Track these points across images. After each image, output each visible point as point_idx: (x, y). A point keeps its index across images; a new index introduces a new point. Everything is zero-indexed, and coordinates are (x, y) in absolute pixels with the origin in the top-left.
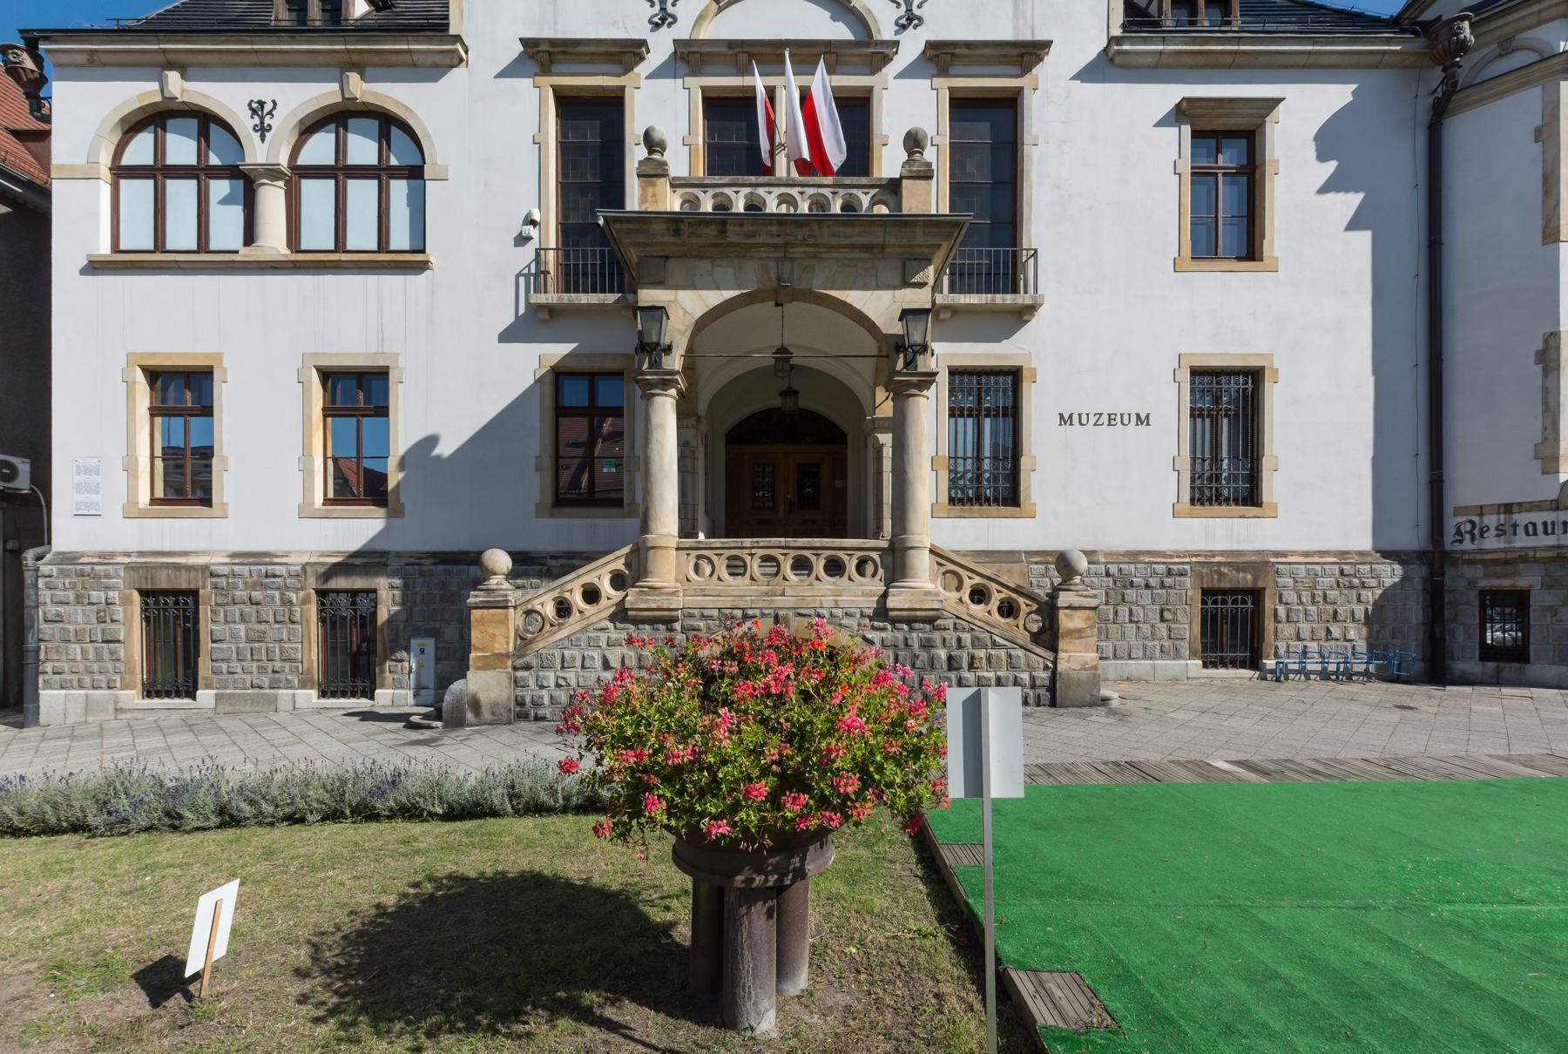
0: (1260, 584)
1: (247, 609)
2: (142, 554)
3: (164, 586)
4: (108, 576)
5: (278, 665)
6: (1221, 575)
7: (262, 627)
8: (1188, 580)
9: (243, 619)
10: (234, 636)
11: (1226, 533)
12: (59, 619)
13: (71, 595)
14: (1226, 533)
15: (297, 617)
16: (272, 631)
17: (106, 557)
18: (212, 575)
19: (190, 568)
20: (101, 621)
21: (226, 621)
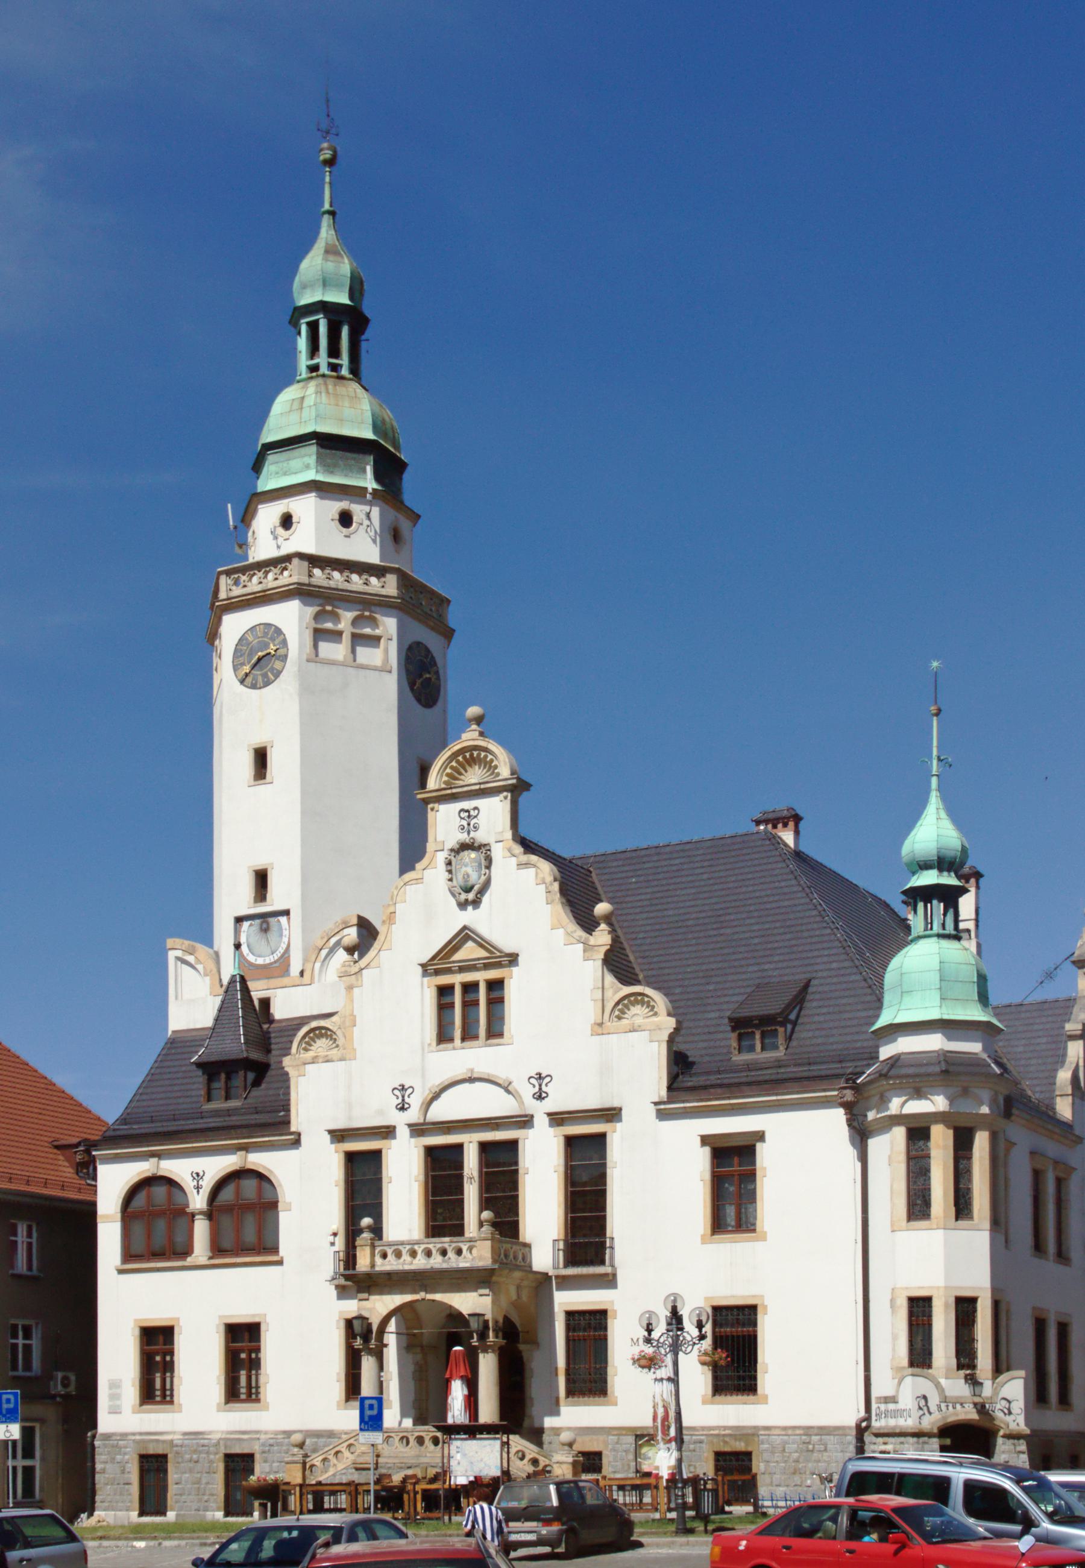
0: (749, 1449)
2: (141, 1434)
3: (151, 1452)
6: (725, 1442)
8: (704, 1445)
11: (734, 1414)
12: (103, 1471)
14: (734, 1414)
17: (124, 1436)
19: (164, 1442)
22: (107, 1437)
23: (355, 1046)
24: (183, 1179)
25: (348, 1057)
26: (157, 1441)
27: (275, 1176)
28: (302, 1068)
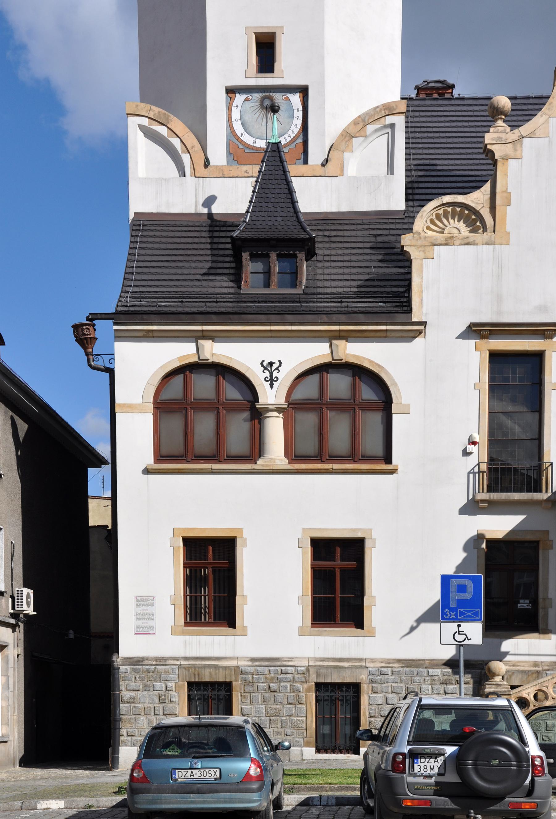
1: (267, 695)
2: (186, 659)
3: (207, 679)
4: (166, 673)
5: (289, 732)
7: (278, 706)
9: (264, 701)
10: (258, 712)
12: (132, 700)
13: (140, 685)
15: (303, 701)
16: (286, 709)
17: (162, 661)
18: (242, 672)
19: (225, 668)
20: (162, 701)
21: (252, 702)
22: (135, 662)
23: (508, 230)
24: (249, 369)
25: (497, 241)
26: (216, 667)
27: (387, 373)
28: (428, 249)
